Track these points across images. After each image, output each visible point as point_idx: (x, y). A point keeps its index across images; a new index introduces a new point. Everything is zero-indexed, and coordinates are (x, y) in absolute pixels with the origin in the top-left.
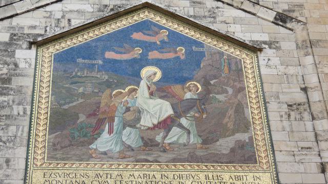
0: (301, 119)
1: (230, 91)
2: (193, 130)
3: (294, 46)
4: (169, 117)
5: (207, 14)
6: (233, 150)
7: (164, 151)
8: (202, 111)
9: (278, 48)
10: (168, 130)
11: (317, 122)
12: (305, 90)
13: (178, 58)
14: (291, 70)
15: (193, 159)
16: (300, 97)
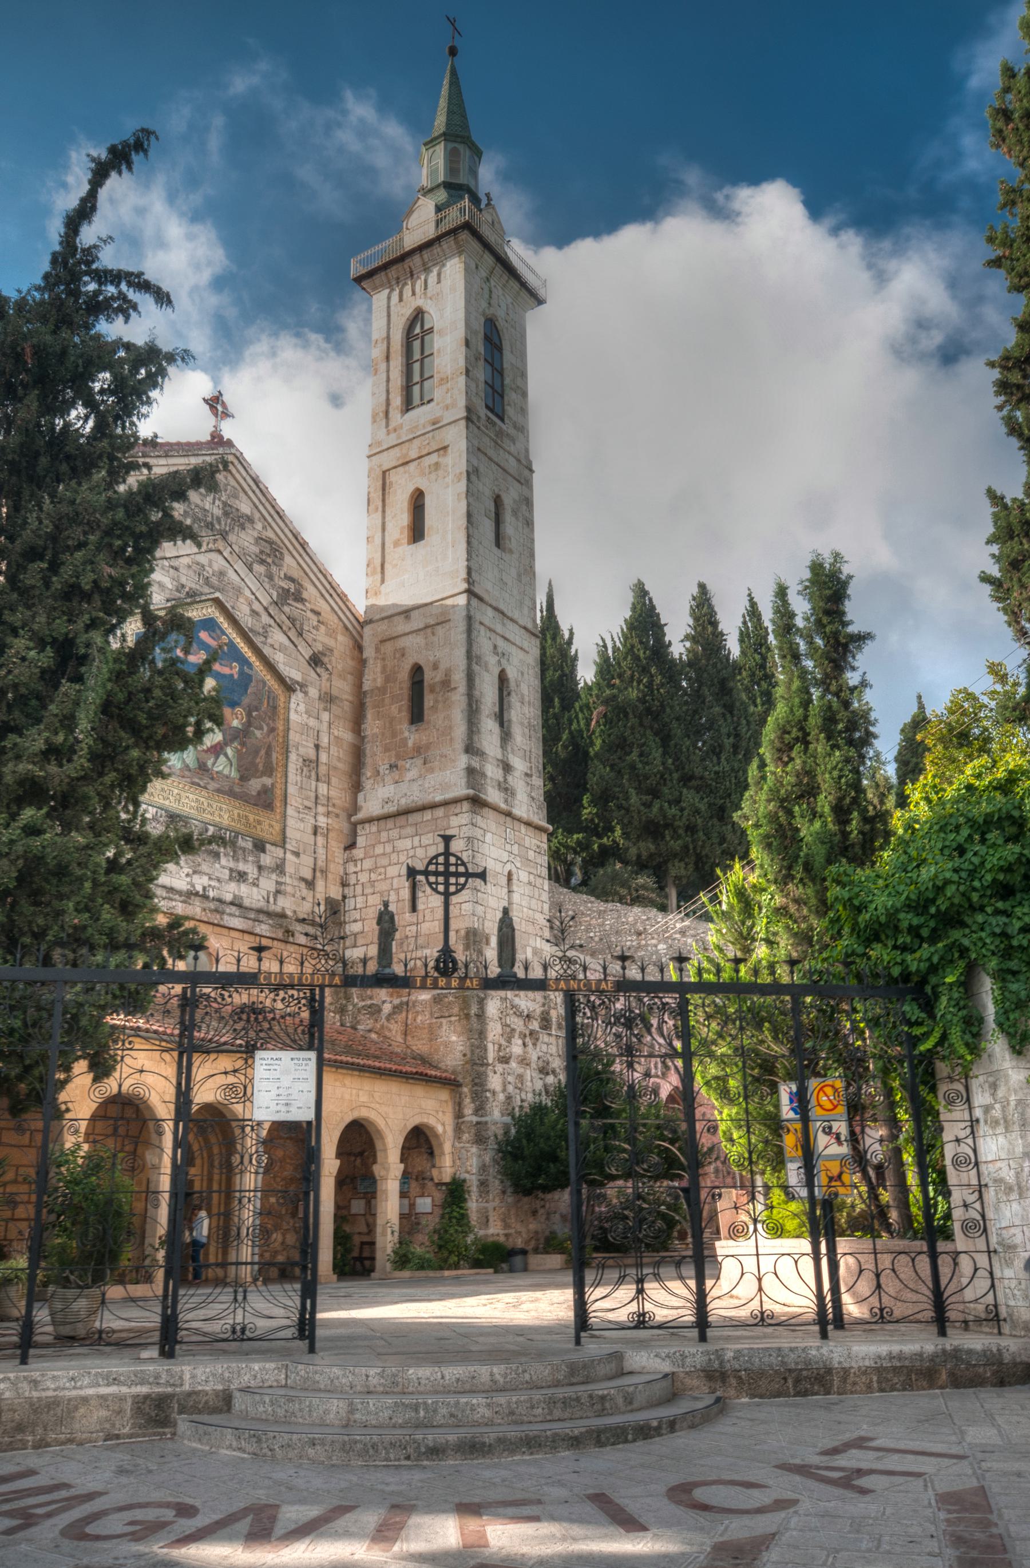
0: (309, 777)
1: (265, 728)
2: (234, 761)
3: (317, 696)
4: (219, 743)
5: (261, 630)
6: (259, 793)
7: (212, 779)
8: (243, 744)
9: (306, 693)
10: (217, 758)
11: (320, 784)
12: (317, 747)
13: (232, 675)
14: (312, 722)
15: (231, 794)
16: (311, 753)
